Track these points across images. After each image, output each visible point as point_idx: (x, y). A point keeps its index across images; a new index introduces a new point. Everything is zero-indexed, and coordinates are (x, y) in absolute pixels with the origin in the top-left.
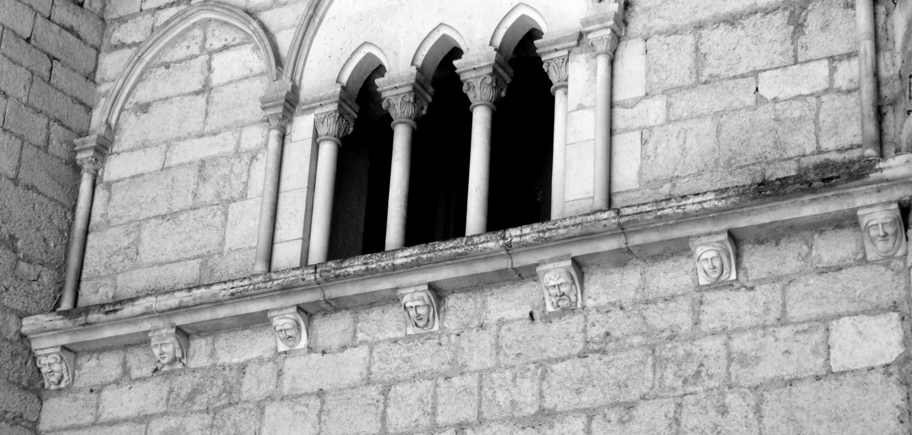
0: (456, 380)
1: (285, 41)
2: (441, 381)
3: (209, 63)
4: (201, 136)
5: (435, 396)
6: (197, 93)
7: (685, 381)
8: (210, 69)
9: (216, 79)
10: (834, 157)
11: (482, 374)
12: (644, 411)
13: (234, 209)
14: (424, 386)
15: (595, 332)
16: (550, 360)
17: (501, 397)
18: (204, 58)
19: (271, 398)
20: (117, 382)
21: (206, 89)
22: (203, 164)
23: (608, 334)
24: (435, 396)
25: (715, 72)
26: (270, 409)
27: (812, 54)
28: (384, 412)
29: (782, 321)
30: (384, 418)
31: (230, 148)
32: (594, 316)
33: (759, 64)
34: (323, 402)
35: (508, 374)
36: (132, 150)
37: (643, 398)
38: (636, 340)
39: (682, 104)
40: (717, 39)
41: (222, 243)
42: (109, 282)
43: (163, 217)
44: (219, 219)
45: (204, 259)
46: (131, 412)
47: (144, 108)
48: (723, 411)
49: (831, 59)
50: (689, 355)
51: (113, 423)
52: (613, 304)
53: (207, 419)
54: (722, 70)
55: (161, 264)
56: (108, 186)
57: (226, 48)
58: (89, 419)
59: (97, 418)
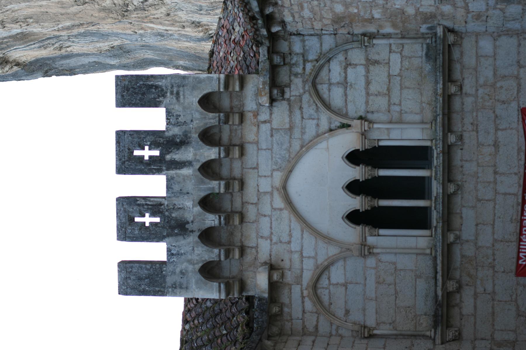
0: (480, 175)
1: (333, 251)
2: (479, 180)
3: (333, 285)
4: (365, 285)
5: (484, 182)
6: (346, 288)
7: (491, 99)
8: (337, 284)
9: (342, 281)
10: (424, 53)
11: (478, 165)
12: (498, 112)
13: (399, 266)
14: (480, 186)
15: (470, 128)
16: (478, 143)
17: (487, 159)
18: (331, 287)
19: (476, 244)
20: (460, 308)
21: (345, 285)
22: (378, 283)
23: (472, 124)
24: (484, 182)
25: (386, 89)
26: (480, 244)
27: (387, 58)
28: (487, 201)
29: (475, 69)
30: (490, 200)
31: (373, 271)
32: (465, 128)
33: (386, 74)
34: (480, 224)
35: (480, 157)
36: (364, 315)
37: (494, 112)
38: (475, 114)
39: (395, 99)
40: (373, 88)
41: (412, 270)
42: (418, 318)
43: (396, 297)
44: (402, 273)
45: (418, 277)
46: (472, 300)
47: (347, 312)
48: (501, 87)
49: (390, 52)
50: (482, 98)
51: (475, 307)
52: (462, 122)
53: (480, 269)
54: (386, 87)
55: (416, 296)
56: (378, 324)
57: (329, 279)
58: (473, 318)
59: (473, 315)
